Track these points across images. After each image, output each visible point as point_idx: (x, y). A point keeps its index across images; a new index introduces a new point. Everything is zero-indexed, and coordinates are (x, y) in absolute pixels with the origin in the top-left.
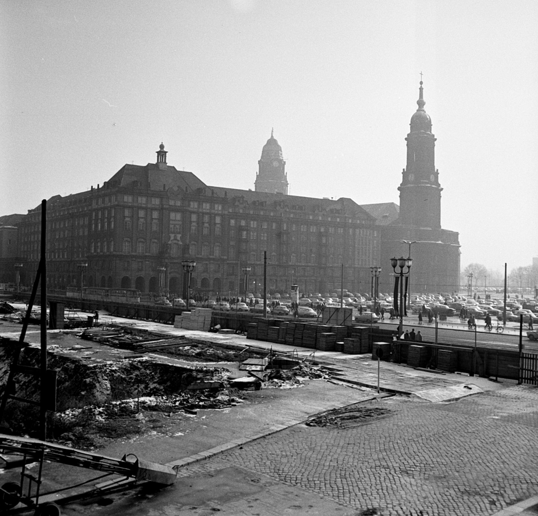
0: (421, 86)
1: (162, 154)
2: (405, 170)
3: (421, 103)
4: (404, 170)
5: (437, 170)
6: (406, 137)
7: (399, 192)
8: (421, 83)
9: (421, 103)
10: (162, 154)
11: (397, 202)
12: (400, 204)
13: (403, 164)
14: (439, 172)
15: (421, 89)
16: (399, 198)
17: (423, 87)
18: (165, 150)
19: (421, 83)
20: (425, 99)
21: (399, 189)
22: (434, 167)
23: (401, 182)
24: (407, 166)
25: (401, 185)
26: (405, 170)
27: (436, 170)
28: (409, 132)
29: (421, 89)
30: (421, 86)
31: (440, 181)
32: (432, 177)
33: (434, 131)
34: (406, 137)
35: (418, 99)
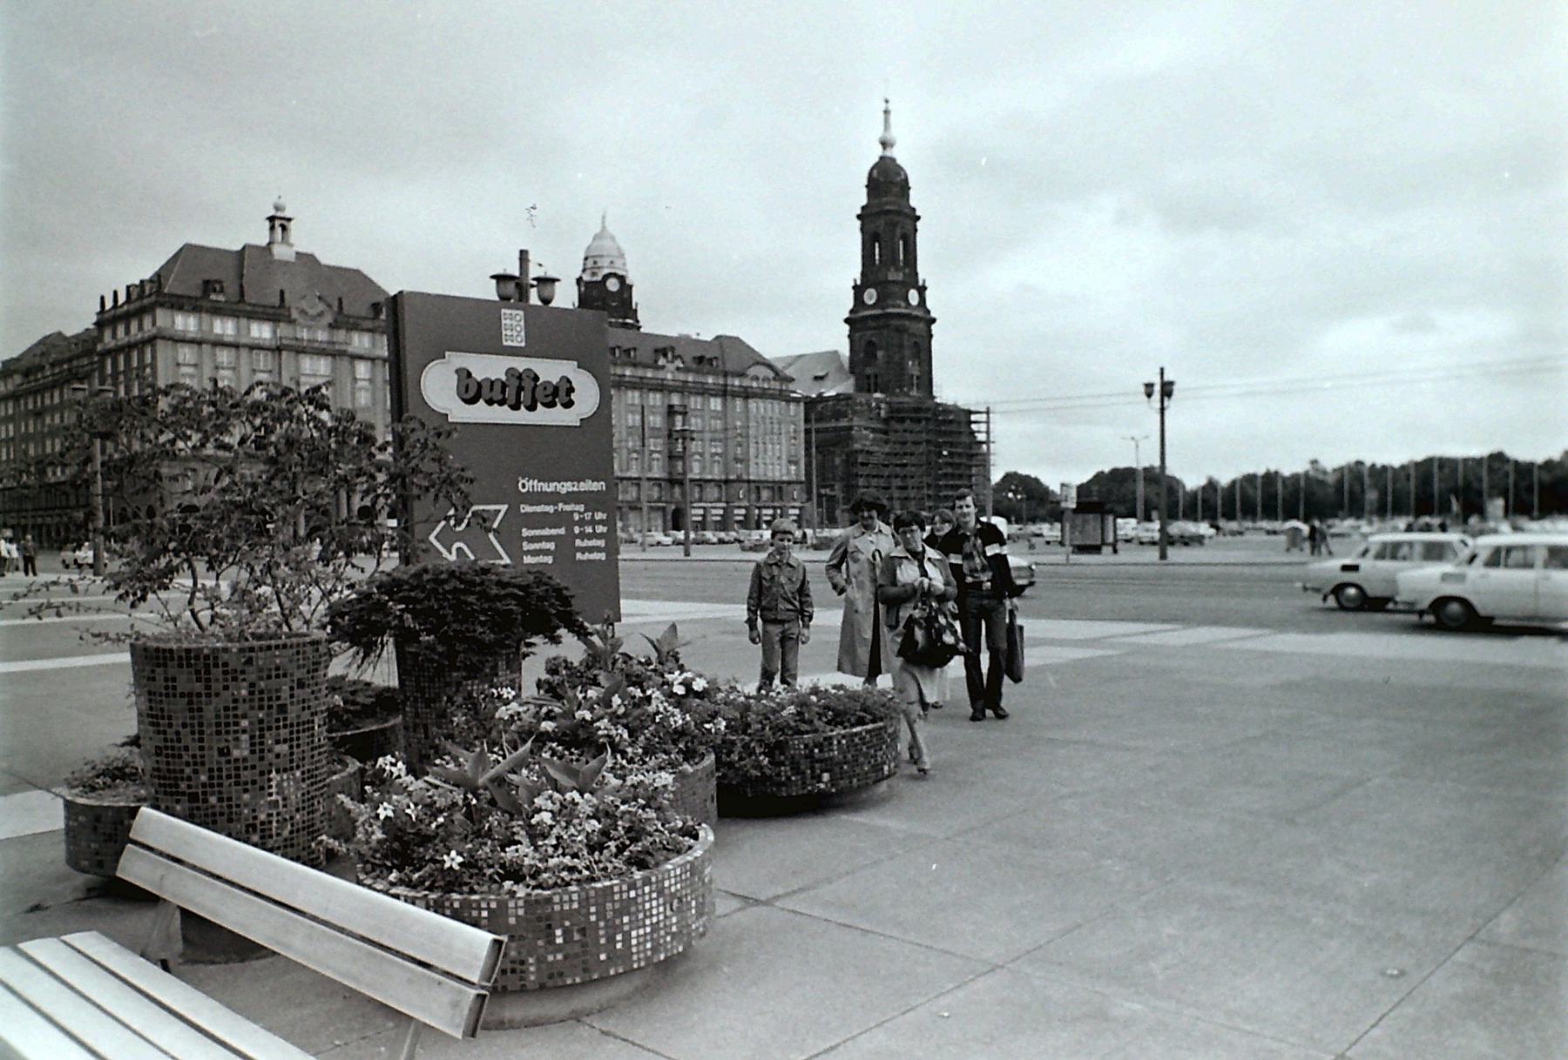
1: (279, 223)
2: (859, 282)
7: (847, 328)
10: (279, 223)
11: (844, 349)
13: (855, 272)
15: (886, 112)
16: (847, 341)
18: (287, 214)
20: (896, 133)
22: (917, 274)
23: (850, 305)
24: (863, 274)
25: (851, 312)
27: (921, 283)
28: (864, 201)
29: (886, 112)
31: (929, 305)
32: (913, 297)
35: (879, 132)
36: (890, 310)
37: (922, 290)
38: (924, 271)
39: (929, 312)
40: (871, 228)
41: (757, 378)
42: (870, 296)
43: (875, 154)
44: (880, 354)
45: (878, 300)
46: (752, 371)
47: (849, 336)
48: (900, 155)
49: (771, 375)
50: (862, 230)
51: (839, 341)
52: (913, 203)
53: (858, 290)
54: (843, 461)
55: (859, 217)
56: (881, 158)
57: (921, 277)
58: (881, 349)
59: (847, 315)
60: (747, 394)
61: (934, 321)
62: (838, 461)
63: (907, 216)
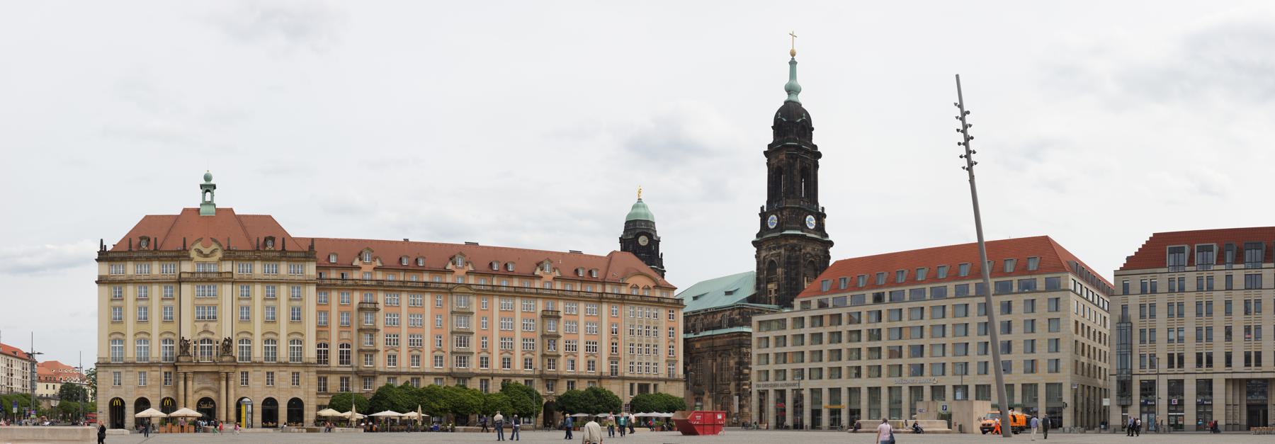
0: (793, 59)
2: (765, 210)
3: (792, 90)
4: (762, 208)
5: (823, 208)
6: (766, 149)
8: (793, 54)
9: (792, 90)
12: (758, 269)
13: (762, 200)
14: (825, 212)
17: (796, 60)
19: (793, 54)
20: (800, 81)
21: (754, 243)
23: (758, 229)
24: (768, 202)
25: (758, 235)
26: (765, 210)
27: (820, 211)
30: (793, 59)
32: (811, 221)
33: (817, 139)
34: (766, 149)
35: (786, 80)
36: (787, 232)
37: (820, 216)
38: (825, 198)
39: (827, 236)
40: (774, 161)
41: (637, 287)
42: (773, 221)
43: (781, 98)
44: (780, 271)
45: (777, 224)
46: (632, 281)
47: (756, 257)
48: (804, 100)
49: (651, 284)
50: (768, 164)
51: (745, 263)
52: (814, 142)
53: (764, 216)
54: (736, 363)
55: (765, 153)
56: (786, 102)
57: (821, 205)
58: (780, 267)
59: (754, 238)
60: (622, 300)
61: (831, 244)
62: (732, 363)
63: (807, 152)
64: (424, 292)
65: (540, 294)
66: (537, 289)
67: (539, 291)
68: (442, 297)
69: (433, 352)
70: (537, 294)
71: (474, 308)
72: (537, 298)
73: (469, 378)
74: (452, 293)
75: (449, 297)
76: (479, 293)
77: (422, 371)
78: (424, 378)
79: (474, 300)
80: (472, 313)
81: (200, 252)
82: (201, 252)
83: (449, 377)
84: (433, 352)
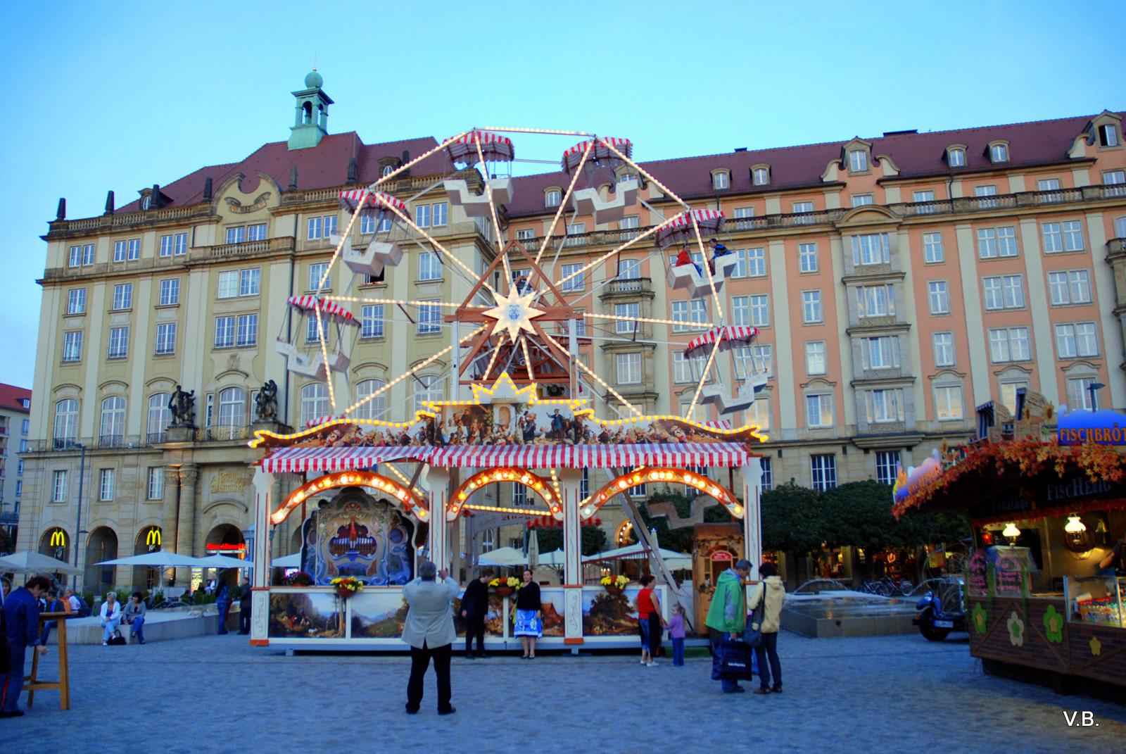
64: (766, 239)
65: (1092, 200)
66: (1080, 189)
67: (1089, 194)
68: (815, 246)
69: (802, 386)
70: (1083, 200)
71: (906, 267)
72: (1084, 211)
73: (909, 448)
74: (838, 232)
75: (834, 242)
76: (912, 222)
77: (777, 438)
78: (780, 454)
79: (903, 240)
80: (901, 276)
81: (235, 204)
82: (238, 204)
83: (850, 450)
84: (802, 386)
